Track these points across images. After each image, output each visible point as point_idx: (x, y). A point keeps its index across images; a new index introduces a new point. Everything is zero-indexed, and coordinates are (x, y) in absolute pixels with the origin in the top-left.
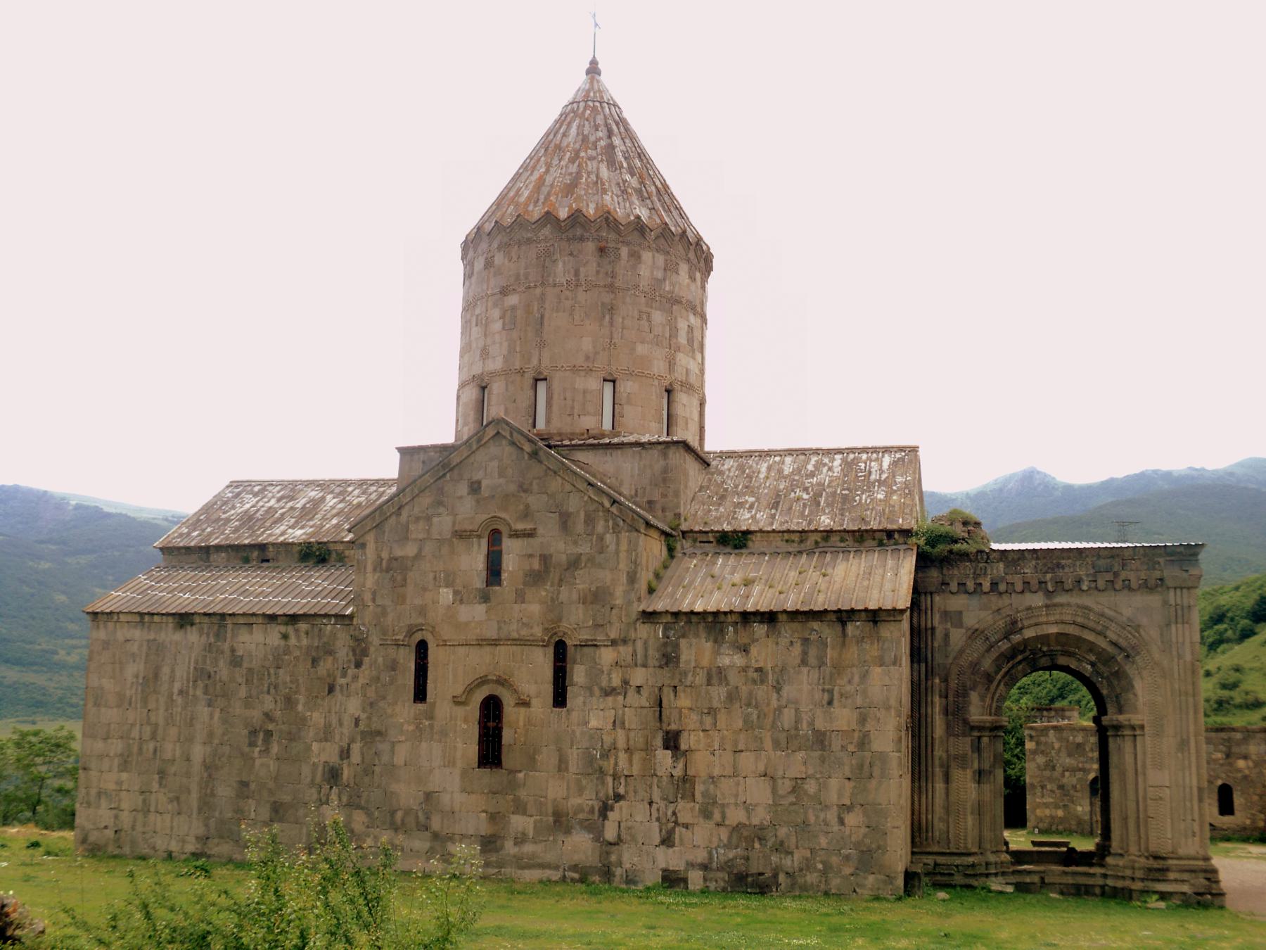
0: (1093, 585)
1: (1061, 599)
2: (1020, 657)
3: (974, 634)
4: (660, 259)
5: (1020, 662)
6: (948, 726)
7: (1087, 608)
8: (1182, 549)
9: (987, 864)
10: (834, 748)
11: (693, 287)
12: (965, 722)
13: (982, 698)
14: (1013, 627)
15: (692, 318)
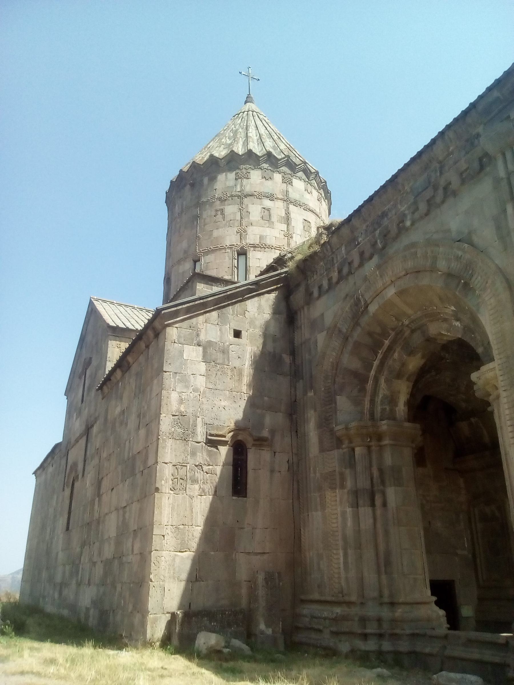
0: (417, 215)
1: (391, 251)
2: (387, 342)
3: (333, 331)
4: (232, 176)
5: (390, 349)
6: (321, 442)
7: (413, 245)
8: (496, 94)
9: (363, 620)
10: (137, 471)
11: (269, 183)
12: (332, 431)
13: (357, 402)
14: (359, 309)
15: (267, 203)
